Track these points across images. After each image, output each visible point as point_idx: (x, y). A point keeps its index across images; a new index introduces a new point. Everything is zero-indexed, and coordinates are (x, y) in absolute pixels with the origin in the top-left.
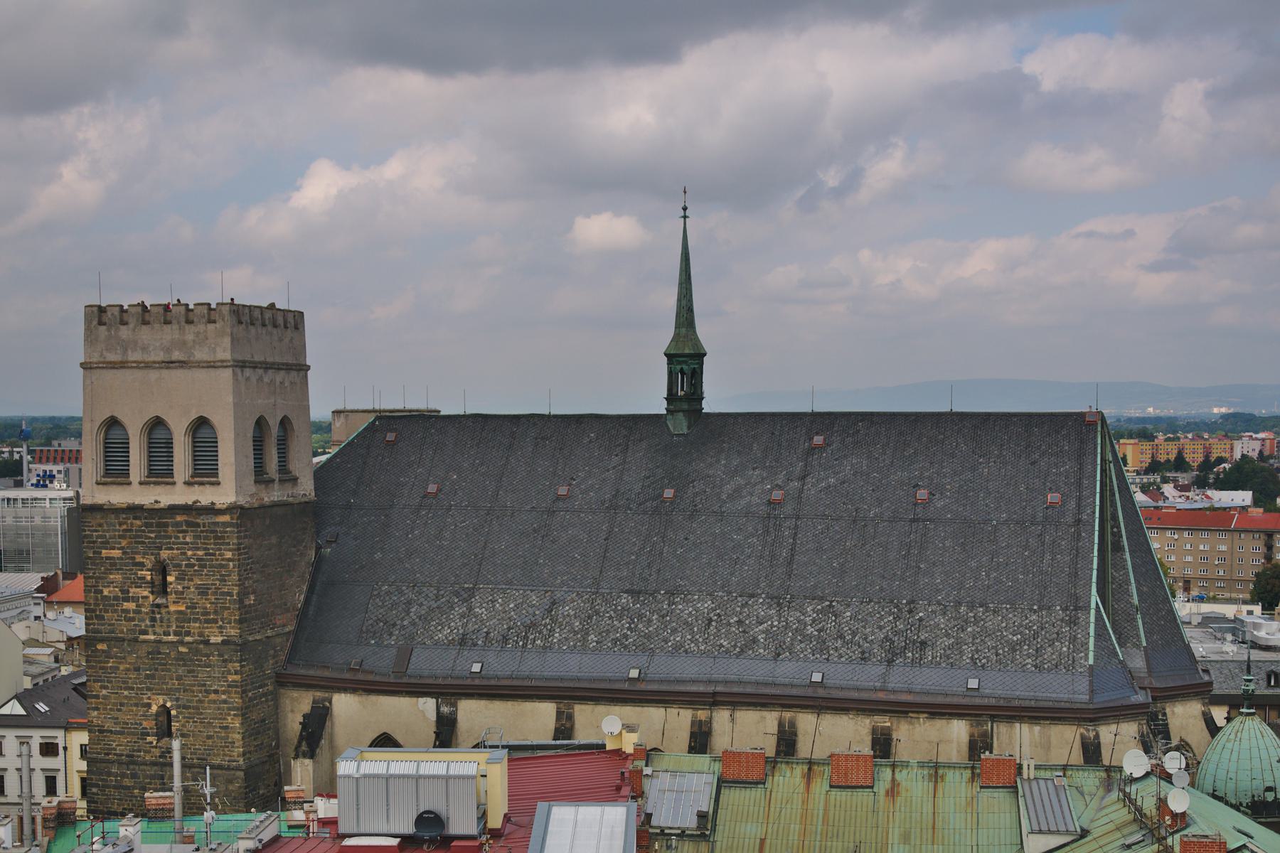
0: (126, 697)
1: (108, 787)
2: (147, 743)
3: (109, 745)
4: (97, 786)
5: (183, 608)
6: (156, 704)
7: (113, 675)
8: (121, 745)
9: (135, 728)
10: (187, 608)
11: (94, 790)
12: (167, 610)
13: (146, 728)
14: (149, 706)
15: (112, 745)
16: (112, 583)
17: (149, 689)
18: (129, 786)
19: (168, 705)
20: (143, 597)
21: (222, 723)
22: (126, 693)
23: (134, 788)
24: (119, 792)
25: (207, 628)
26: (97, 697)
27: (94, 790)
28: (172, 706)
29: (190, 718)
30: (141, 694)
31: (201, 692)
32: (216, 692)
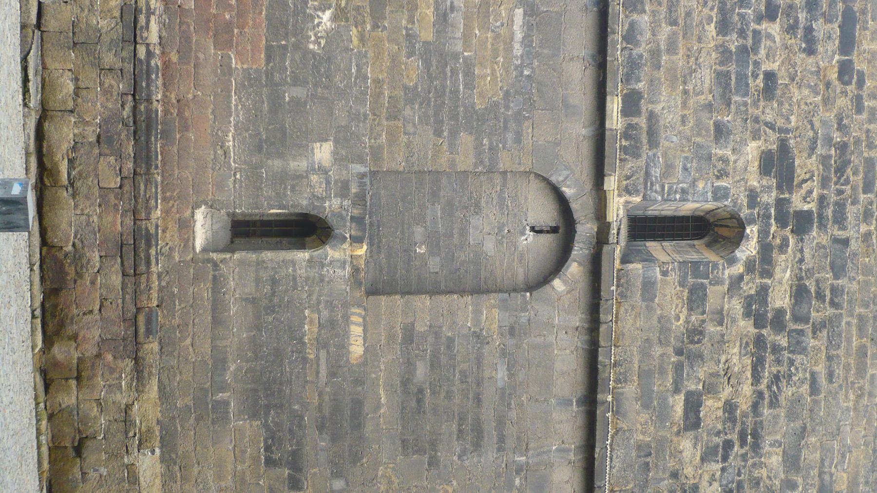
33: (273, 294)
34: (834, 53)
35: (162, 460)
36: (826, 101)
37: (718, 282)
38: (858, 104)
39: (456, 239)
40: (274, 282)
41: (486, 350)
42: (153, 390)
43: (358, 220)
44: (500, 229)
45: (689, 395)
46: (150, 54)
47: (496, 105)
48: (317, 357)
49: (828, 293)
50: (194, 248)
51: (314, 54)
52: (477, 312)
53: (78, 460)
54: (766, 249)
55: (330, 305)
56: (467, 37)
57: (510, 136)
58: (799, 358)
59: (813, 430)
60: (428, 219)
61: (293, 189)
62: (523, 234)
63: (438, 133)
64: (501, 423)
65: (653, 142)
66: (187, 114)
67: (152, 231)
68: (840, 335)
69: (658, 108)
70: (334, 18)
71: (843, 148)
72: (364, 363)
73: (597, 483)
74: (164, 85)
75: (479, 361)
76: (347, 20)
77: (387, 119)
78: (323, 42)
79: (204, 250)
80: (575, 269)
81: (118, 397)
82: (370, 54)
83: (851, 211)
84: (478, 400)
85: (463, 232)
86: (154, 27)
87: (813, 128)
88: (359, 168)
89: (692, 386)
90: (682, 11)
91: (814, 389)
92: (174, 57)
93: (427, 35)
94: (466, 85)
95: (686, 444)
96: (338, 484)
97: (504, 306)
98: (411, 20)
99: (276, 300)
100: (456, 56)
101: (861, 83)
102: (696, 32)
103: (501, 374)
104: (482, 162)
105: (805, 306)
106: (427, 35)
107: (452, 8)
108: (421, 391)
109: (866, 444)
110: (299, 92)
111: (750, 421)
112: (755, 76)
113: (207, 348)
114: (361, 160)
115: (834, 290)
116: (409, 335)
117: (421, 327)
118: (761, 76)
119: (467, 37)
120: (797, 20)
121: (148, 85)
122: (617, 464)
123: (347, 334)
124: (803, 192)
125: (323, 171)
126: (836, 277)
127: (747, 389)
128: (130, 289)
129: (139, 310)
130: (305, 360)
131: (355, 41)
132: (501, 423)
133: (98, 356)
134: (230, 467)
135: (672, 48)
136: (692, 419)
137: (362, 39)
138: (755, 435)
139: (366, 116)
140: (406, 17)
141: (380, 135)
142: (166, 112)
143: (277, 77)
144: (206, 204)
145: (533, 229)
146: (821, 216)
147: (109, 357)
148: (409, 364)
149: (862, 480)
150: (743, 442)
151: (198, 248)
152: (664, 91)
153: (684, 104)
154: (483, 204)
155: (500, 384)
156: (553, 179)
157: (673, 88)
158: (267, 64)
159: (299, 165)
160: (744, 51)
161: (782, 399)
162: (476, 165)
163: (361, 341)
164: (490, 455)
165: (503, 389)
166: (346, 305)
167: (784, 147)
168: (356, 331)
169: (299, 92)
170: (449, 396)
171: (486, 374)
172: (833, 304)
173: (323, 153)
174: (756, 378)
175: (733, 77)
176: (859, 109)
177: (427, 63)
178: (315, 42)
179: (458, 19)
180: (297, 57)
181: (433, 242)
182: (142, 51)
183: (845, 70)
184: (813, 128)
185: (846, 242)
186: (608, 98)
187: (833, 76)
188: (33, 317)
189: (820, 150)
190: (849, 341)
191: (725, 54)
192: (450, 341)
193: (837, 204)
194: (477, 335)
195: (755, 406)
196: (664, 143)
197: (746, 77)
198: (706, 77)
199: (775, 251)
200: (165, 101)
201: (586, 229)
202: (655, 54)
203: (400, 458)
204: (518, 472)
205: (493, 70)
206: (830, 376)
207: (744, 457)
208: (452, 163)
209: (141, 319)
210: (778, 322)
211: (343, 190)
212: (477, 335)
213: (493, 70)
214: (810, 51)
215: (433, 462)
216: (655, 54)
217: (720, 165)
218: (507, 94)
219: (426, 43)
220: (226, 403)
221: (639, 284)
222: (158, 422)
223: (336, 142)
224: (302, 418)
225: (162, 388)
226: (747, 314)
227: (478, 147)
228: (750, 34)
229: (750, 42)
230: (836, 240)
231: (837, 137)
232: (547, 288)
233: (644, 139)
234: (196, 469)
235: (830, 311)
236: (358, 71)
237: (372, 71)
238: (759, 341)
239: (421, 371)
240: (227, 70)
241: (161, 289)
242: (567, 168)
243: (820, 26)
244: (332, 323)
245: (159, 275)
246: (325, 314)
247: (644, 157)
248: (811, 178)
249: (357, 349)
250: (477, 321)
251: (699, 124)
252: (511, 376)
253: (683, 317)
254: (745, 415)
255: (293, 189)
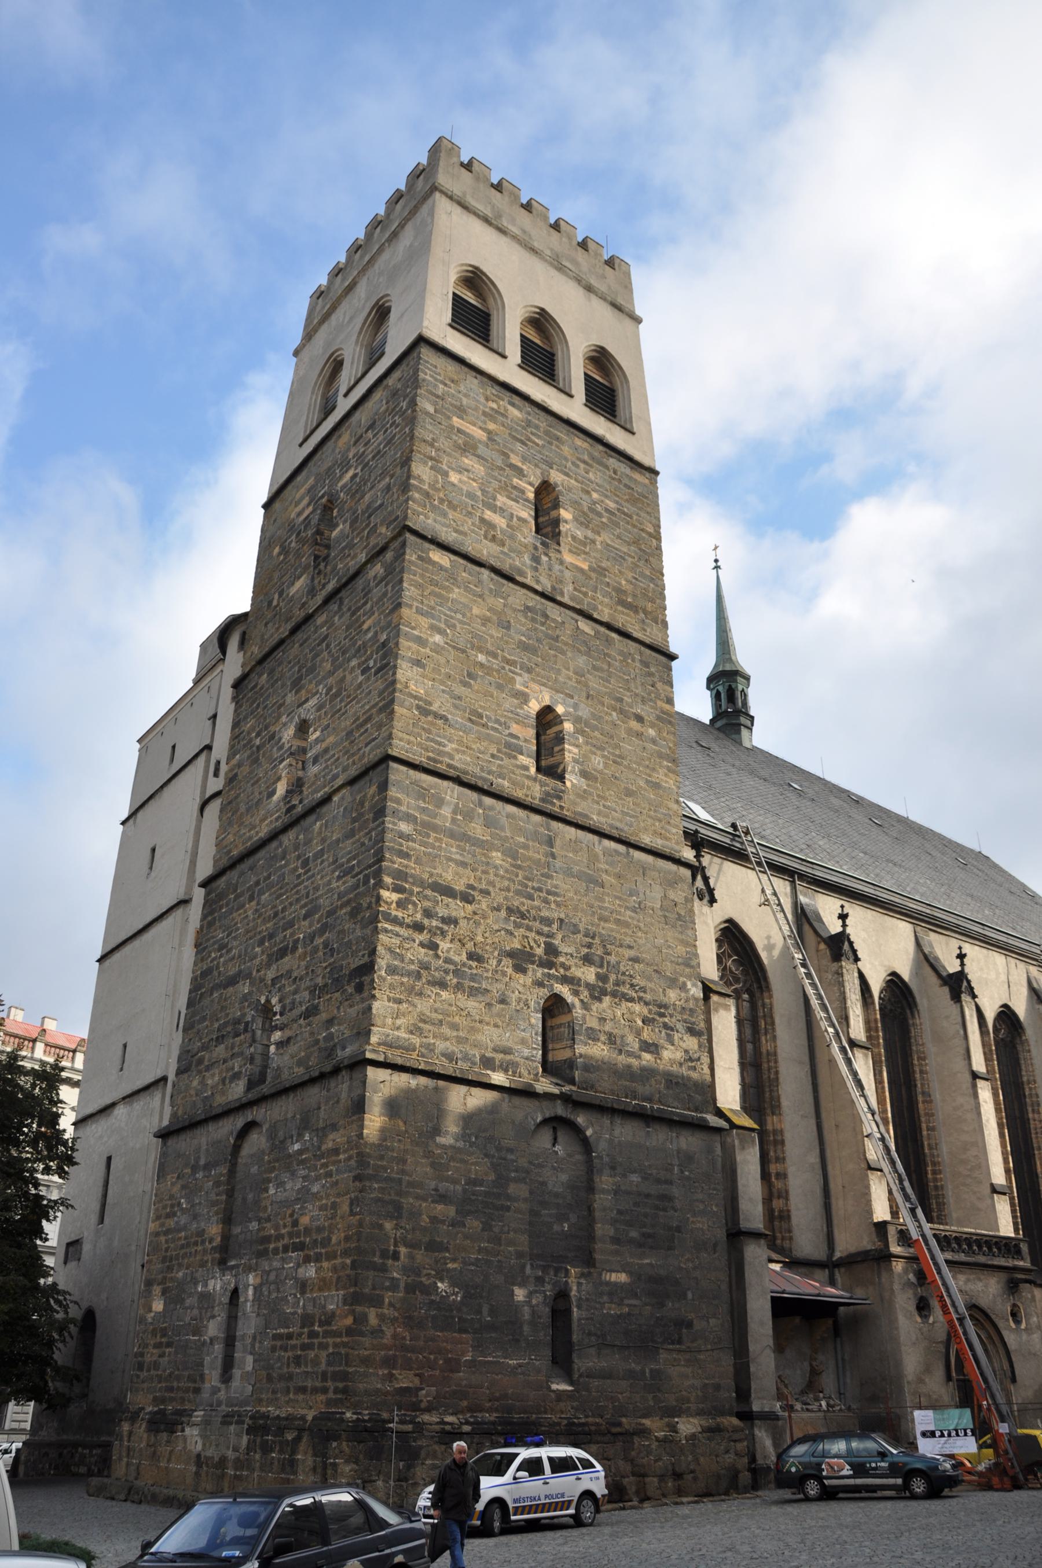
0: (482, 665)
1: (435, 828)
2: (518, 766)
3: (440, 744)
4: (409, 818)
5: (585, 566)
6: (537, 700)
7: (460, 616)
8: (464, 753)
9: (494, 729)
10: (591, 569)
11: (404, 827)
12: (558, 556)
13: (517, 737)
14: (524, 698)
15: (444, 746)
16: (468, 471)
17: (529, 671)
18: (483, 841)
19: (560, 709)
20: (520, 519)
21: (650, 776)
22: (481, 658)
23: (492, 847)
24: (458, 847)
25: (623, 613)
26: (421, 642)
27: (404, 827)
28: (567, 713)
29: (598, 748)
30: (510, 671)
31: (615, 710)
32: (640, 719)
33: (595, 1335)
34: (456, 904)
35: (679, 1416)
36: (484, 917)
37: (584, 1018)
38: (486, 893)
39: (560, 1201)
40: (590, 1334)
41: (623, 1188)
42: (647, 1422)
43: (557, 1270)
44: (554, 1168)
45: (641, 1049)
46: (467, 1423)
47: (492, 1164)
48: (629, 1305)
49: (587, 939)
50: (571, 1391)
51: (463, 1297)
52: (603, 1191)
53: (685, 1476)
54: (565, 980)
55: (602, 1294)
56: (455, 1182)
57: (510, 1157)
58: (622, 969)
59: (657, 965)
60: (550, 1220)
61: (540, 1317)
62: (556, 1153)
63: (508, 1209)
64: (658, 1181)
65: (507, 1051)
66: (497, 1395)
67: (565, 1422)
68: (609, 936)
69: (491, 1045)
70: (442, 1280)
71: (510, 910)
72: (630, 1273)
73: (690, 1120)
74: (480, 1411)
75: (628, 1193)
76: (443, 1270)
77: (500, 1245)
78: (456, 1290)
79: (571, 1384)
80: (581, 1120)
81: (653, 1447)
82: (463, 1255)
83: (545, 913)
84: (648, 1196)
85: (557, 1195)
86: (449, 1419)
87: (499, 931)
88: (528, 1267)
89: (637, 1046)
90: (434, 1015)
91: (635, 960)
92: (465, 1403)
93: (451, 1211)
94: (481, 1185)
95: (666, 1054)
96: (690, 1295)
97: (600, 1172)
98: (443, 1222)
99: (599, 1333)
100: (465, 1191)
101: (471, 887)
102: (446, 1006)
103: (635, 1178)
104: (524, 1179)
105: (596, 959)
106: (451, 1211)
107: (436, 1190)
108: (643, 1235)
109: (663, 929)
110: (485, 1309)
111: (655, 1009)
112: (471, 968)
113: (624, 1384)
114: (523, 1267)
115: (586, 935)
116: (615, 1240)
117: (612, 1232)
118: (471, 962)
119: (455, 1182)
120: (437, 928)
121: (486, 1423)
122: (676, 1104)
123: (616, 1284)
124: (535, 946)
125: (530, 1294)
126: (579, 932)
127: (637, 1008)
128: (599, 1438)
129: (609, 1432)
130: (629, 1314)
131: (455, 1265)
132: (658, 1181)
133: (632, 1461)
134: (683, 1369)
135: (455, 1027)
136: (652, 1049)
137: (454, 1260)
138: (660, 1006)
139: (499, 1261)
140: (441, 1226)
141: (510, 1252)
142: (496, 1410)
143: (477, 1326)
144: (547, 1381)
145: (554, 1145)
146: (548, 936)
147: (633, 1453)
148: (631, 1241)
149: (680, 936)
150: (662, 1015)
151: (570, 1388)
152: (479, 1037)
153: (488, 1024)
154: (541, 1179)
155: (639, 1180)
156: (533, 1128)
157: (478, 1031)
158: (469, 1333)
159: (526, 1313)
160: (456, 973)
161: (642, 984)
162: (526, 1183)
163: (619, 1275)
164: (675, 1191)
165: (642, 1178)
166: (601, 1283)
167: (511, 954)
168: (614, 1277)
169: (485, 1309)
170: (646, 1215)
171: (635, 1189)
172: (593, 938)
173: (520, 1294)
174: (631, 1000)
175: (472, 984)
176: (488, 893)
177: (469, 1213)
178: (457, 1296)
179: (444, 1186)
180: (465, 1309)
181: (562, 1218)
182: (467, 1428)
183: (467, 899)
184: (499, 931)
185: (561, 921)
186: (493, 1082)
187: (469, 908)
188: (624, 1509)
189: (511, 927)
190: (612, 930)
191: (459, 987)
192: (620, 1212)
193: (541, 923)
194: (616, 1192)
195: (646, 1004)
196: (510, 1044)
197: (471, 974)
198: (472, 1005)
199: (568, 974)
200: (490, 1410)
201: (560, 1110)
202: (460, 1040)
203: (677, 1252)
204: (682, 1172)
205: (472, 1164)
206: (630, 947)
207: (671, 1016)
208: (525, 1200)
209: (615, 1430)
210: (602, 978)
211: (540, 1280)
212: (616, 1192)
213: (472, 1164)
214: (455, 922)
215: (678, 1229)
216: (460, 1040)
217: (522, 1005)
218: (486, 1155)
219: (457, 1212)
220: (651, 1371)
221: (586, 1075)
222: (661, 1419)
223: (514, 1284)
224: (658, 1318)
225: (645, 1416)
226: (600, 1000)
227: (517, 1180)
228: (447, 966)
229: (452, 967)
230: (560, 928)
231: (503, 913)
232: (591, 1140)
233: (508, 1057)
234: (684, 1393)
235: (597, 941)
236: (473, 1264)
237: (473, 1254)
238: (614, 994)
239: (634, 1234)
240: (472, 1364)
241: (593, 1416)
242: (527, 1118)
243: (442, 912)
244: (610, 1294)
245: (586, 1417)
246: (605, 1298)
247: (518, 1059)
248: (527, 937)
249: (622, 1278)
250: (607, 1192)
251: (499, 1015)
252: (634, 1172)
253: (603, 1047)
254: (650, 1011)
255: (540, 1317)
